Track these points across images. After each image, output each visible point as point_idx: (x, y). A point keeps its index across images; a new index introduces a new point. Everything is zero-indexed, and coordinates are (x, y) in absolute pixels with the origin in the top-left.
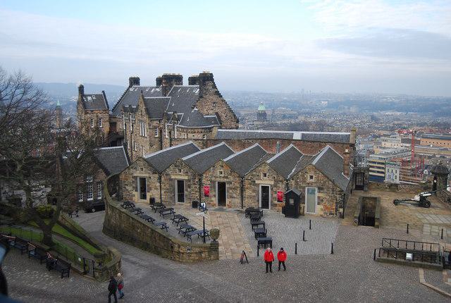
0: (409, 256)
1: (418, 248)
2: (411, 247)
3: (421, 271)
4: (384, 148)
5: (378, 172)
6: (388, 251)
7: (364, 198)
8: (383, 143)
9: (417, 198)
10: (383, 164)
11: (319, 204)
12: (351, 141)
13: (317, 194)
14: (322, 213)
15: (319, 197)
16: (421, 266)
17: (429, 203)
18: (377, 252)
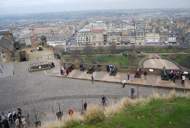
0: (40, 67)
1: (42, 64)
2: (40, 64)
3: (45, 71)
4: (23, 33)
5: (23, 42)
6: (33, 68)
7: (20, 52)
8: (22, 32)
9: (38, 48)
10: (24, 39)
11: (4, 58)
12: (10, 33)
13: (2, 55)
14: (6, 61)
15: (3, 56)
16: (44, 69)
17: (42, 49)
18: (29, 69)
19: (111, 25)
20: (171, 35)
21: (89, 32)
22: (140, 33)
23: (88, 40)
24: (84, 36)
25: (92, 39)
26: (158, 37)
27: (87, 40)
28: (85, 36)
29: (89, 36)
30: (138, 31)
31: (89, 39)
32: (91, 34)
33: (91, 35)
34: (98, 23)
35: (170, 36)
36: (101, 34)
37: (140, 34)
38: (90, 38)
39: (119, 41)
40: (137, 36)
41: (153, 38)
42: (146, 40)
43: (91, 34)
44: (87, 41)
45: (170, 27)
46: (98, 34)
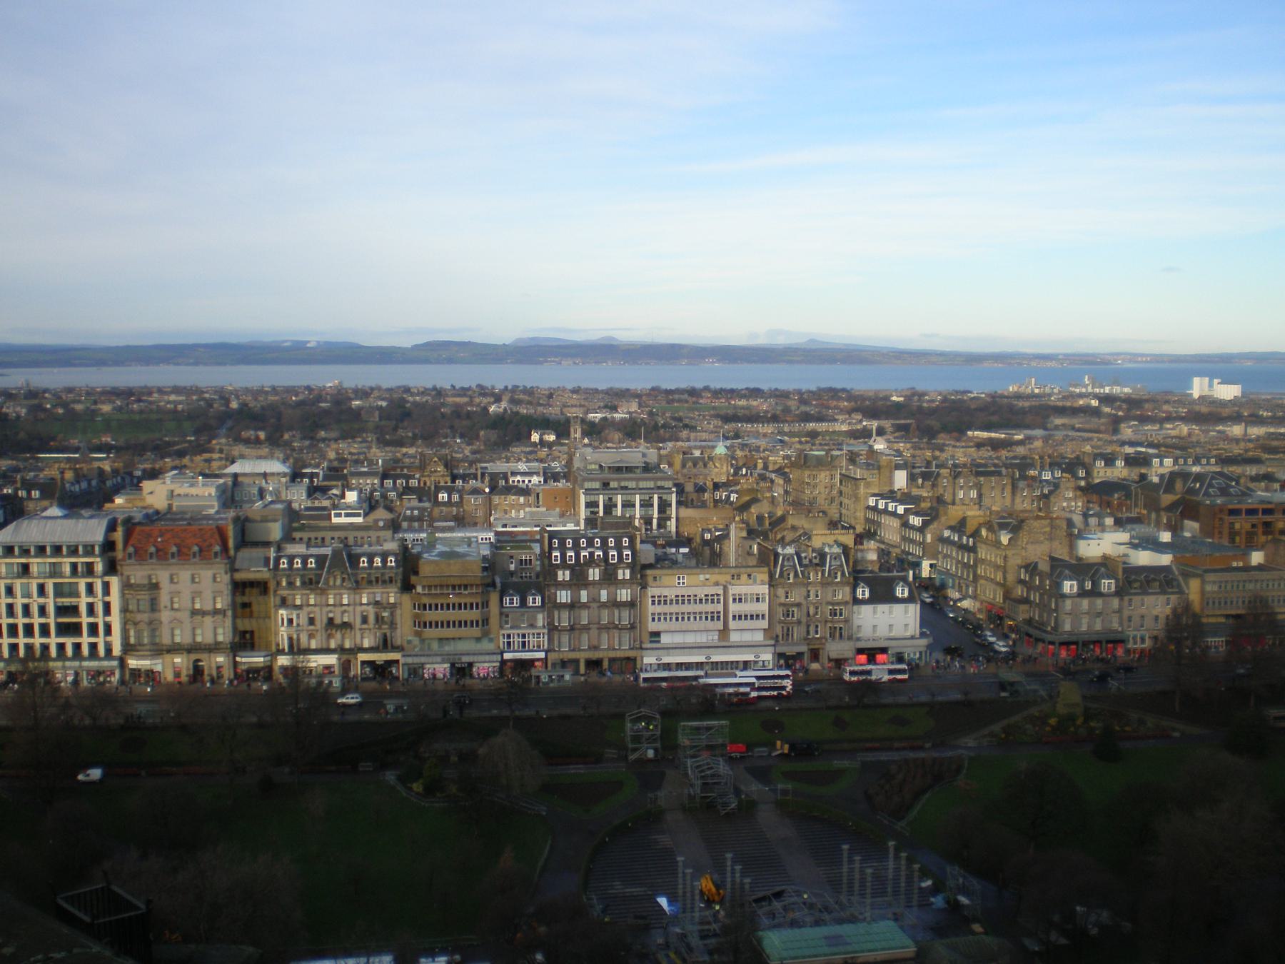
19: (351, 497)
20: (872, 583)
21: (89, 550)
22: (591, 561)
23: (74, 629)
24: (42, 590)
25: (115, 619)
26: (764, 607)
27: (64, 630)
28: (50, 589)
29: (90, 589)
30: (576, 547)
31: (85, 620)
32: (112, 568)
33: (115, 582)
34: (236, 476)
35: (863, 592)
36: (206, 574)
37: (594, 574)
38: (99, 608)
39: (385, 645)
40: (564, 596)
41: (714, 617)
42: (653, 627)
43: (112, 568)
44: (69, 642)
45: (885, 520)
46: (184, 575)
